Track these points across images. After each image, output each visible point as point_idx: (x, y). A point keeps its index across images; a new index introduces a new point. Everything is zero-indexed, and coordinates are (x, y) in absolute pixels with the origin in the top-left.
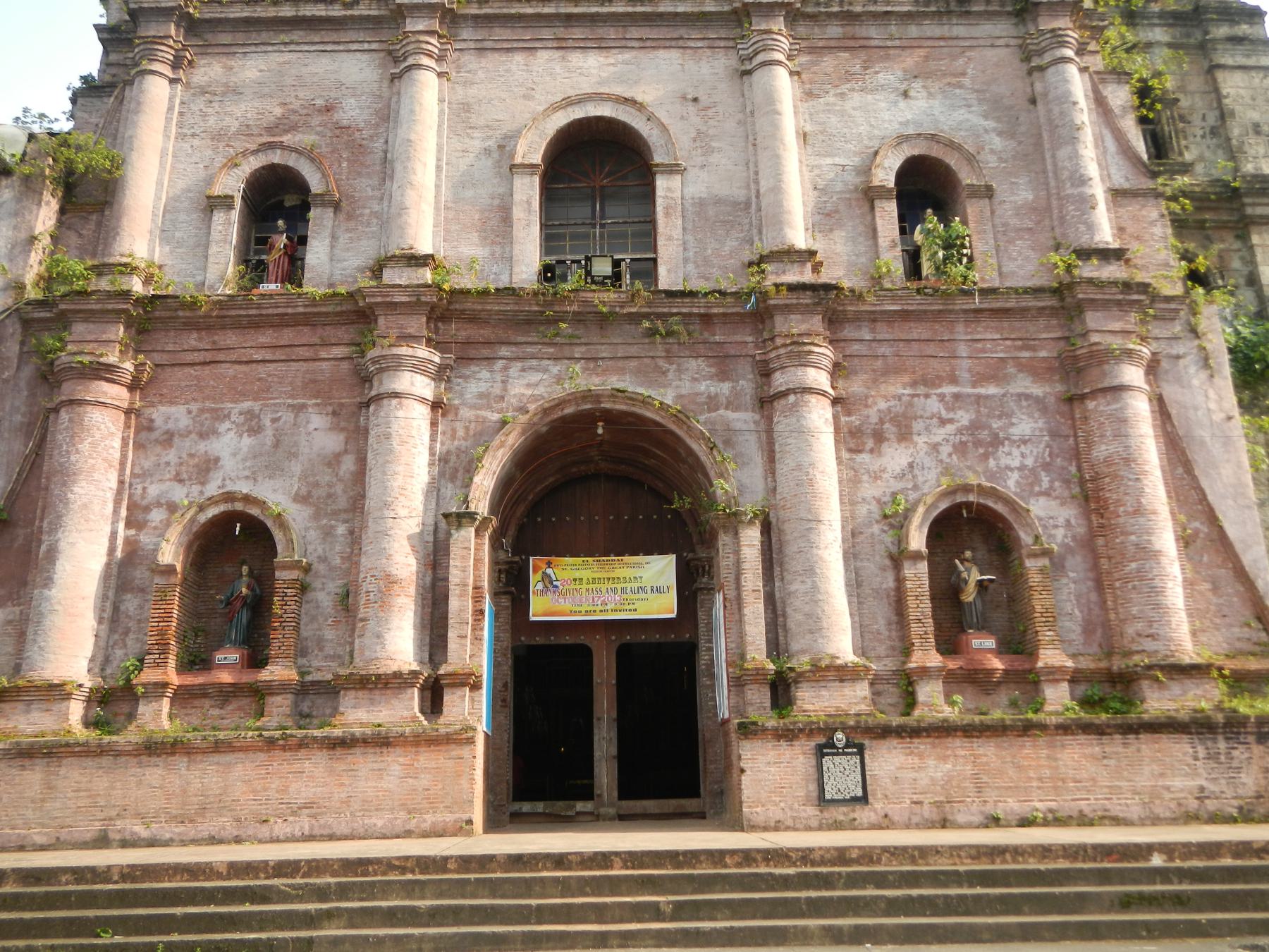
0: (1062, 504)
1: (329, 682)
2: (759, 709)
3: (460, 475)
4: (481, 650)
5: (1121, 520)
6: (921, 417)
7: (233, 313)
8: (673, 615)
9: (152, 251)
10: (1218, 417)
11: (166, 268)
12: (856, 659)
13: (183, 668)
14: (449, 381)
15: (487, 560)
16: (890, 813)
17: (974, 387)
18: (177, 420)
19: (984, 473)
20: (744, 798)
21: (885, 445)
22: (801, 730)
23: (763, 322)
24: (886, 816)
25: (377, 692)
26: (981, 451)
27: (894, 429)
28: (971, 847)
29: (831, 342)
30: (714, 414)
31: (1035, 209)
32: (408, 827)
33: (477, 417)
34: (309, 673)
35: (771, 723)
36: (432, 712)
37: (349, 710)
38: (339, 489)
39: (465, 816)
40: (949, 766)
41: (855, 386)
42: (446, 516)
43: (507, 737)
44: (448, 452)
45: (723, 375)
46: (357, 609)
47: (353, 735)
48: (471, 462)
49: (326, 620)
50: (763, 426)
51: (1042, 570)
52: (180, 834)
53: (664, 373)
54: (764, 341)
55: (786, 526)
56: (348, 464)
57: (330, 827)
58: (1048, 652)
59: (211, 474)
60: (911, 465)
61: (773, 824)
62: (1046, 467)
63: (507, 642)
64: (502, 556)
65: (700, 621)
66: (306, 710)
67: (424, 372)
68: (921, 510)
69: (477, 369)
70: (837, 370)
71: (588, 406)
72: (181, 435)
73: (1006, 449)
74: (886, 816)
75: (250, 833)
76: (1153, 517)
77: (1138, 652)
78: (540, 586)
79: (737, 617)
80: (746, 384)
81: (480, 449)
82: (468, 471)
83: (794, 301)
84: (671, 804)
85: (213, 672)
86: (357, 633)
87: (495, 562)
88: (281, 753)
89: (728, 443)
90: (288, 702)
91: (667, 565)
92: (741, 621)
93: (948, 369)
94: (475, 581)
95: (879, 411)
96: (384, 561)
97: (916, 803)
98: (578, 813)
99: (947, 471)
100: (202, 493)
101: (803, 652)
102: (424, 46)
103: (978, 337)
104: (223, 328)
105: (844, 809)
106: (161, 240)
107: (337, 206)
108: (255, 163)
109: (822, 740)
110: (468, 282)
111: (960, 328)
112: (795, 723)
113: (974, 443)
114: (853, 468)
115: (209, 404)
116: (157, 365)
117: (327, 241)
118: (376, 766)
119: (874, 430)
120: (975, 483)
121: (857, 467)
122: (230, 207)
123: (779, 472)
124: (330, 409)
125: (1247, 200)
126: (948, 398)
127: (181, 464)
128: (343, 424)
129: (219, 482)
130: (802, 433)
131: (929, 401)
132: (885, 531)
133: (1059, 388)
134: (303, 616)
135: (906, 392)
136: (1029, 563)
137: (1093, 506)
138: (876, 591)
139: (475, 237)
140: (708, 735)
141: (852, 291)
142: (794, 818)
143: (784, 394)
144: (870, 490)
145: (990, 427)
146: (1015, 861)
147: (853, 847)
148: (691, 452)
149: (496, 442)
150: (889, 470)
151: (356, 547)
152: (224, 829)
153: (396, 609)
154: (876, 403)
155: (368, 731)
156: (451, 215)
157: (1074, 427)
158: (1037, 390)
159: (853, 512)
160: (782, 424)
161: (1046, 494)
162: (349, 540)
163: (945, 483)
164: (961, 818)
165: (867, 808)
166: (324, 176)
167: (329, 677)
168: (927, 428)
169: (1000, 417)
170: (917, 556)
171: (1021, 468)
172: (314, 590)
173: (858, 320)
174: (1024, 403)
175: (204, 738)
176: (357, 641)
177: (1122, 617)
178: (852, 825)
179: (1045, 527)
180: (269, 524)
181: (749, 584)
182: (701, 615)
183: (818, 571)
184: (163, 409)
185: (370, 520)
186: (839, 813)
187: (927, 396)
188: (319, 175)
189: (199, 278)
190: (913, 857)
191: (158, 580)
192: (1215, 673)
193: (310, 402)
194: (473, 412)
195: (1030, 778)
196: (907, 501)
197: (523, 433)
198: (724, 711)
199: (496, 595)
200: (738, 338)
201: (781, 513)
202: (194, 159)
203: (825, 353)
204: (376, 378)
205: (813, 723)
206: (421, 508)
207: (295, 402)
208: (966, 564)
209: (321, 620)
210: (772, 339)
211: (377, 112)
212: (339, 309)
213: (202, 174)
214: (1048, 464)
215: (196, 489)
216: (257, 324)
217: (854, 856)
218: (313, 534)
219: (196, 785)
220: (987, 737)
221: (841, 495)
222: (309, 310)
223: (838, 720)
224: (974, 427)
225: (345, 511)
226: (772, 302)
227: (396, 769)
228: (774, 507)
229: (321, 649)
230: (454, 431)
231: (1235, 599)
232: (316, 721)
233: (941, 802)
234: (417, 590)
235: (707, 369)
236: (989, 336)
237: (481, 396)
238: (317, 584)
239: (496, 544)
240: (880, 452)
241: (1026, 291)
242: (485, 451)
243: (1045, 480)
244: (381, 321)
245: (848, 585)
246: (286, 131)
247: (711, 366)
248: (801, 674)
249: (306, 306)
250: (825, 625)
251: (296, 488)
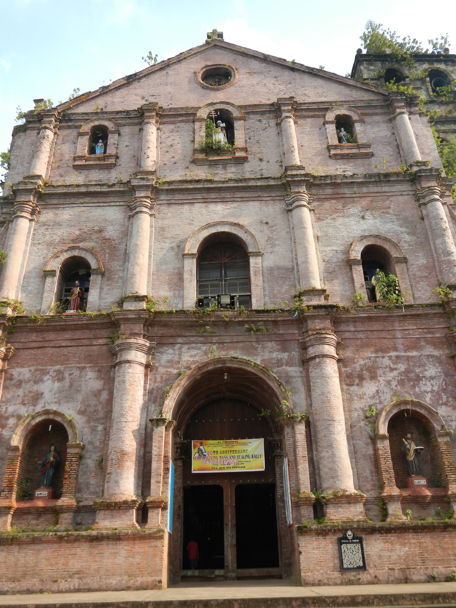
1: (91, 506)
2: (308, 519)
3: (158, 400)
4: (167, 489)
6: (381, 367)
7: (53, 324)
8: (263, 470)
9: (17, 296)
11: (23, 304)
12: (356, 492)
13: (20, 499)
14: (153, 354)
15: (171, 442)
16: (378, 575)
17: (405, 352)
18: (24, 375)
19: (414, 394)
20: (302, 567)
21: (364, 382)
22: (330, 530)
23: (302, 324)
24: (376, 577)
25: (115, 511)
26: (412, 383)
27: (368, 374)
28: (421, 594)
29: (335, 332)
30: (280, 368)
31: (428, 267)
32: (128, 585)
33: (167, 371)
34: (81, 501)
35: (314, 527)
36: (142, 522)
37: (101, 521)
38: (100, 408)
39: (158, 579)
40: (407, 549)
41: (348, 354)
42: (151, 421)
43: (180, 534)
44: (153, 389)
45: (284, 350)
46: (106, 469)
47: (102, 534)
48: (163, 393)
49: (91, 474)
50: (304, 374)
51: (446, 443)
52: (12, 588)
53: (256, 349)
54: (303, 333)
55: (318, 424)
56: (105, 395)
57: (89, 584)
58: (453, 486)
59: (39, 401)
60: (377, 391)
61: (317, 582)
62: (444, 390)
63: (180, 485)
64: (178, 440)
65: (277, 472)
66: (79, 521)
67: (142, 351)
68: (384, 414)
69: (167, 349)
70: (338, 346)
71: (220, 366)
72: (26, 382)
73: (424, 382)
74: (376, 577)
75: (48, 587)
78: (197, 455)
79: (295, 470)
80: (296, 354)
81: (168, 388)
82: (162, 398)
83: (317, 314)
84: (264, 571)
85: (34, 501)
86: (106, 480)
87: (175, 443)
88: (66, 544)
89: (288, 382)
90: (70, 517)
91: (260, 443)
92: (297, 473)
93: (392, 344)
94: (165, 453)
95: (360, 365)
96: (121, 443)
97: (391, 569)
98: (216, 576)
99: (395, 394)
100: (34, 410)
101: (329, 488)
102: (144, 203)
103: (406, 328)
104: (48, 331)
105: (354, 573)
106: (22, 291)
107: (103, 274)
108: (66, 256)
109: (341, 535)
110: (163, 308)
111: (397, 324)
112: (326, 526)
113: (408, 380)
114: (349, 394)
115: (39, 367)
116: (16, 349)
117: (98, 290)
118: (113, 551)
119: (358, 374)
120: (409, 399)
121: (351, 393)
122: (54, 276)
123: (313, 396)
124: (97, 369)
126: (393, 358)
127: (25, 396)
128: (102, 376)
129: (42, 405)
130: (324, 377)
131: (384, 359)
132: (366, 425)
133: (447, 351)
134: (80, 472)
135: (373, 355)
136: (440, 440)
138: (364, 456)
139: (166, 287)
140: (282, 533)
141: (344, 308)
142: (328, 579)
143: (314, 358)
144: (358, 404)
145: (414, 372)
146: (444, 602)
147: (359, 596)
148: (270, 387)
149: (175, 384)
150: (367, 394)
151: (107, 436)
152: (35, 585)
153: (125, 468)
154: (358, 361)
155: (110, 532)
156: (155, 277)
158: (436, 353)
159: (350, 415)
160: (313, 373)
161: (445, 404)
162: (104, 433)
163: (395, 399)
164: (415, 578)
165: (366, 573)
166: (98, 261)
167: (92, 503)
168: (384, 373)
169: (419, 367)
170: (383, 437)
171: (432, 392)
172: (86, 458)
173: (347, 321)
174: (431, 360)
175: (28, 536)
176: (106, 485)
178: (358, 582)
179: (446, 421)
180: (66, 425)
181: (300, 453)
182: (277, 469)
183: (334, 446)
184: (18, 369)
185: (114, 423)
186: (351, 576)
187: (383, 357)
188: (95, 261)
189: (38, 308)
190: (390, 601)
191: (10, 454)
193: (87, 366)
194: (165, 369)
195: (450, 554)
196: (377, 409)
197: (188, 379)
198: (290, 521)
199: (175, 460)
200: (291, 331)
201: (315, 416)
202: (39, 254)
203: (332, 337)
204: (119, 354)
205: (335, 526)
206: (139, 417)
207: (81, 365)
208: (408, 441)
209: (88, 474)
210: (307, 332)
211: (122, 232)
212: (102, 321)
213: (42, 261)
214: (445, 389)
215: (31, 408)
216: (64, 329)
217: (360, 600)
218: (86, 430)
219: (22, 561)
220: (426, 532)
221: (344, 407)
222: (89, 322)
223: (348, 524)
224: (407, 371)
225: (102, 418)
226: (306, 314)
227: (123, 553)
228: (312, 413)
229: (88, 489)
230: (156, 378)
232: (84, 527)
233: (404, 569)
234: (136, 458)
235: (276, 347)
236: (411, 328)
237: (168, 361)
238: (87, 455)
239: (175, 434)
240: (362, 385)
241: (427, 305)
242: (170, 388)
243: (444, 397)
244: (122, 327)
245: (350, 452)
246: (81, 241)
247: (278, 345)
248: (329, 500)
249: (87, 320)
250: (339, 474)
251: (79, 407)
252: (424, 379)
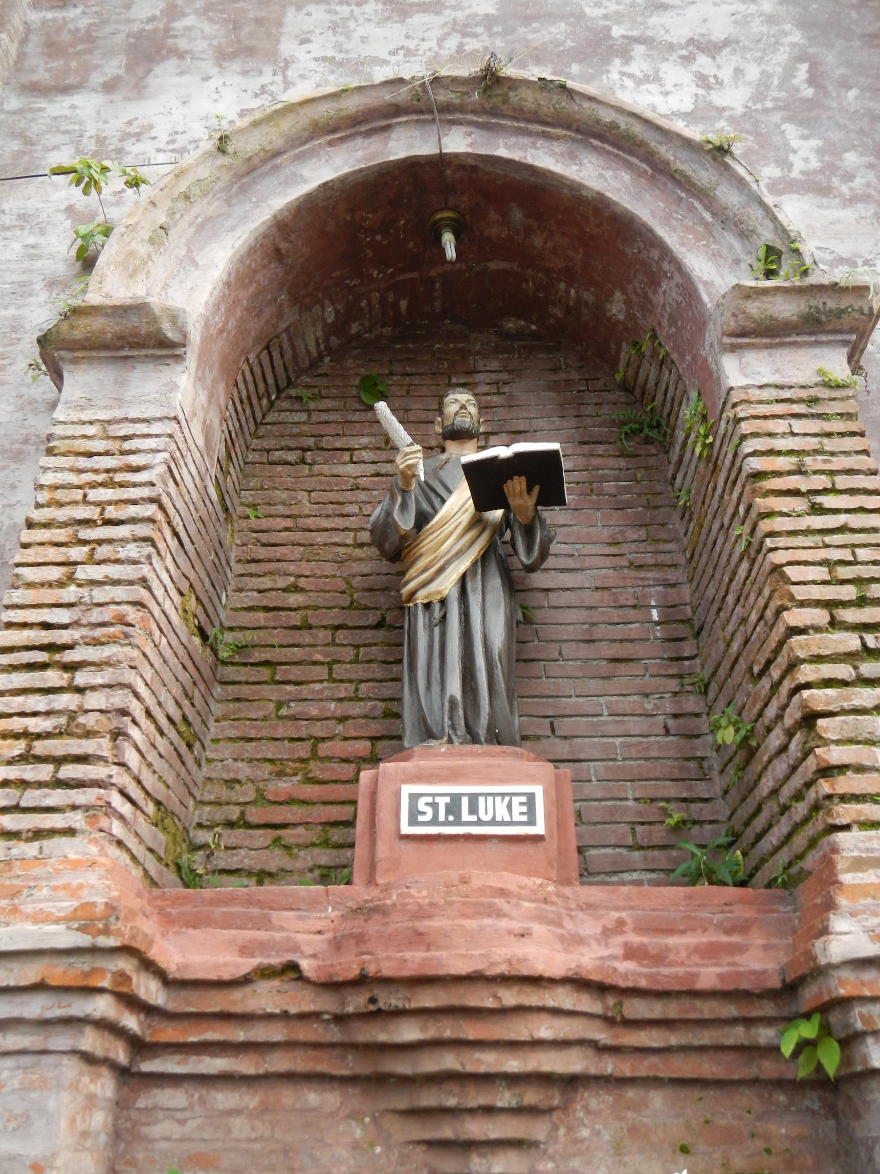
119: (139, 36)
150: (162, 132)
214: (811, 104)
252: (639, 50)
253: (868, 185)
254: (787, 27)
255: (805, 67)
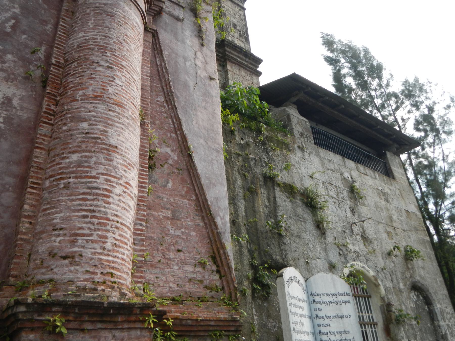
0: (7, 79)
5: (76, 105)
10: (203, 74)
76: (117, 109)
77: (41, 283)
125: (227, 49)
137: (48, 89)
157: (58, 18)
177: (39, 228)
192: (152, 319)
231: (193, 234)
253: (9, 67)
254: (16, 6)
255: (13, 21)
